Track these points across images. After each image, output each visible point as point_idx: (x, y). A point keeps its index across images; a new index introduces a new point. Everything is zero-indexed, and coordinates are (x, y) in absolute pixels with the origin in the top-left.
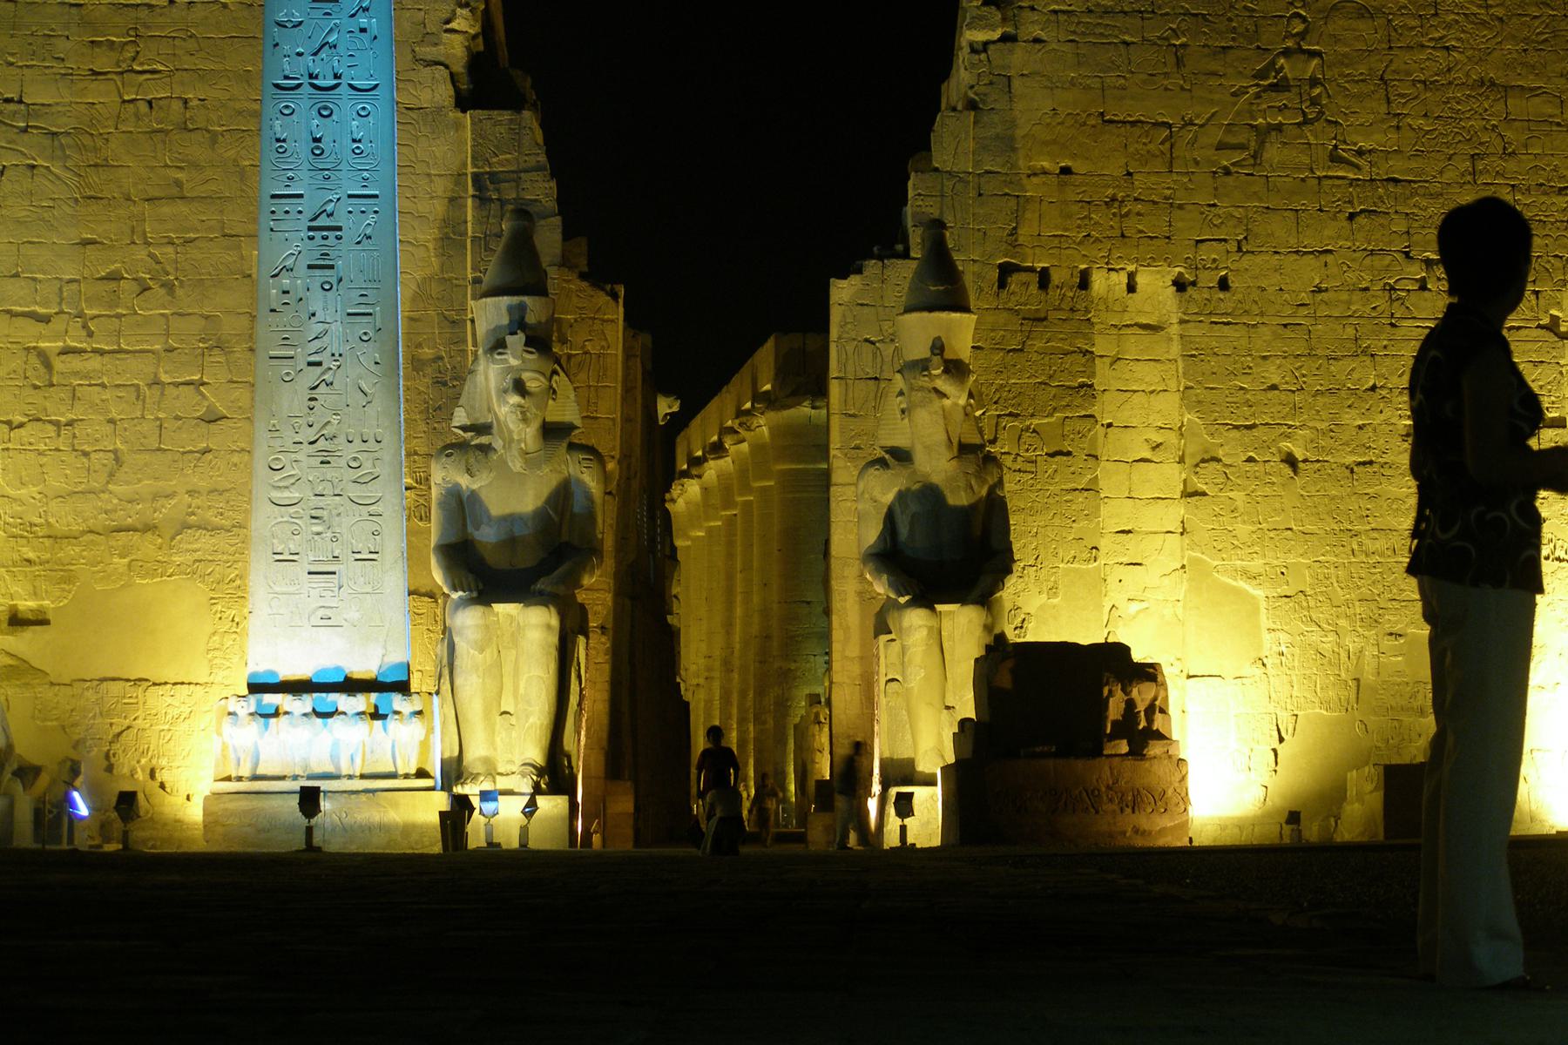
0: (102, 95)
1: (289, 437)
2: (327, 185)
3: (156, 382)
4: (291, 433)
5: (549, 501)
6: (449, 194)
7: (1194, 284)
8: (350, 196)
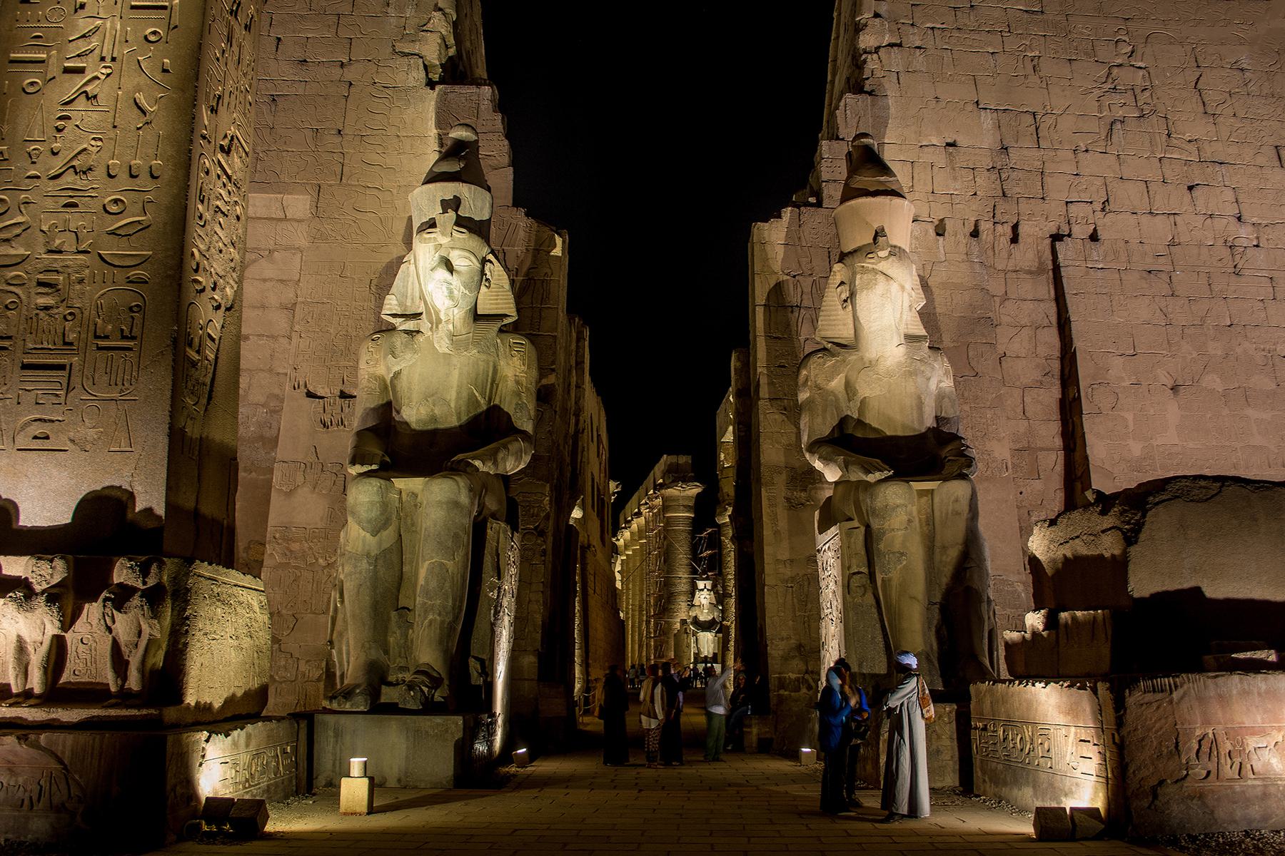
7: (1069, 235)
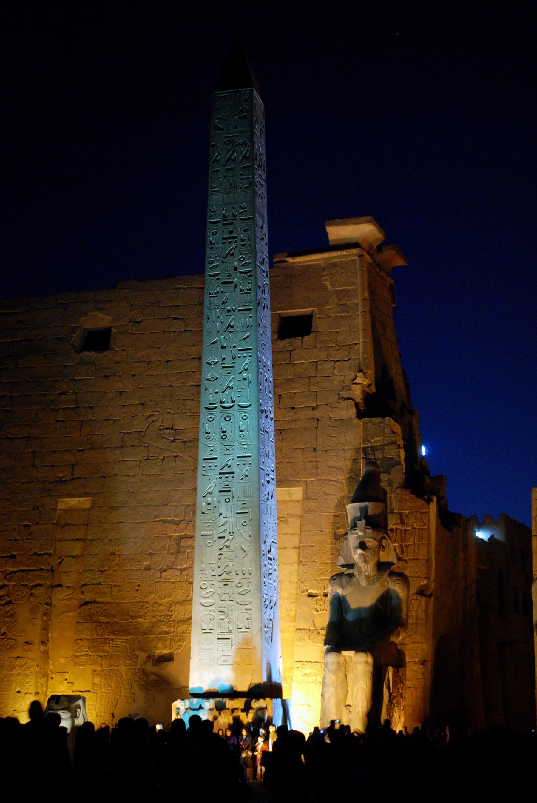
1: (209, 573)
2: (228, 452)
4: (210, 571)
5: (377, 601)
6: (353, 458)
8: (238, 457)
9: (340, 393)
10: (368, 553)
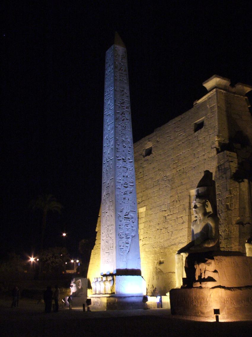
0: (174, 171)
3: (177, 218)
9: (212, 146)
10: (197, 209)
